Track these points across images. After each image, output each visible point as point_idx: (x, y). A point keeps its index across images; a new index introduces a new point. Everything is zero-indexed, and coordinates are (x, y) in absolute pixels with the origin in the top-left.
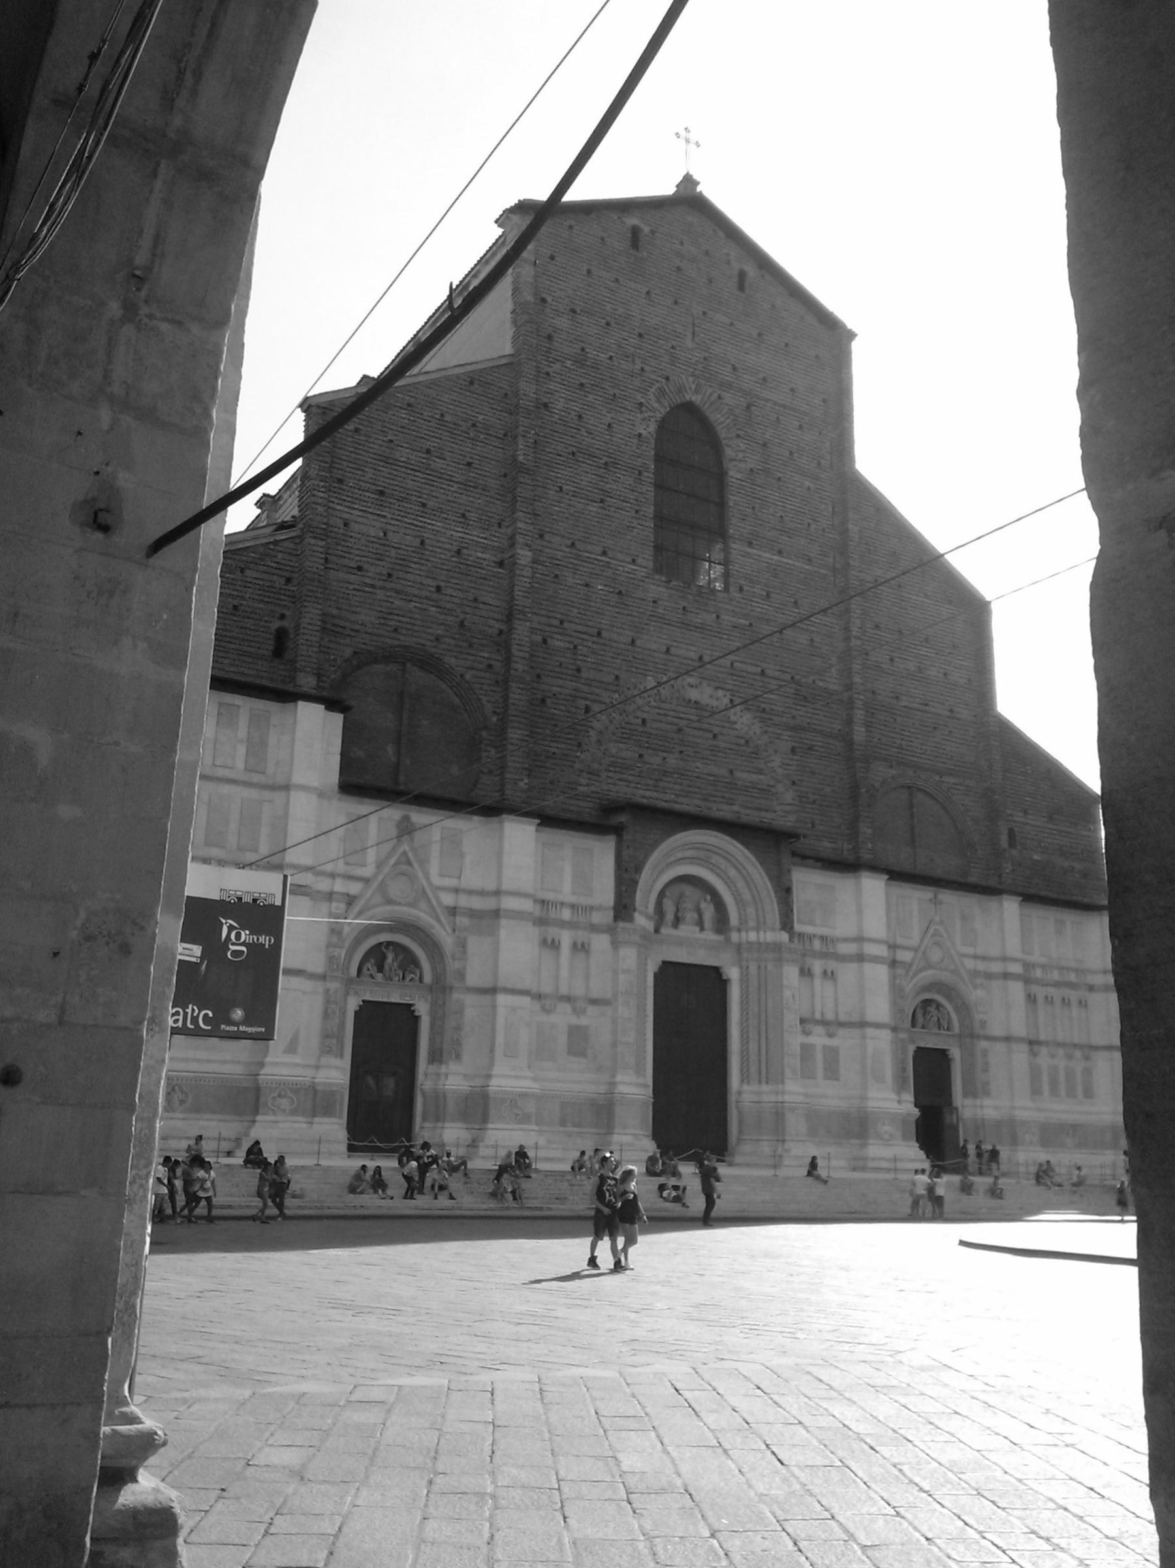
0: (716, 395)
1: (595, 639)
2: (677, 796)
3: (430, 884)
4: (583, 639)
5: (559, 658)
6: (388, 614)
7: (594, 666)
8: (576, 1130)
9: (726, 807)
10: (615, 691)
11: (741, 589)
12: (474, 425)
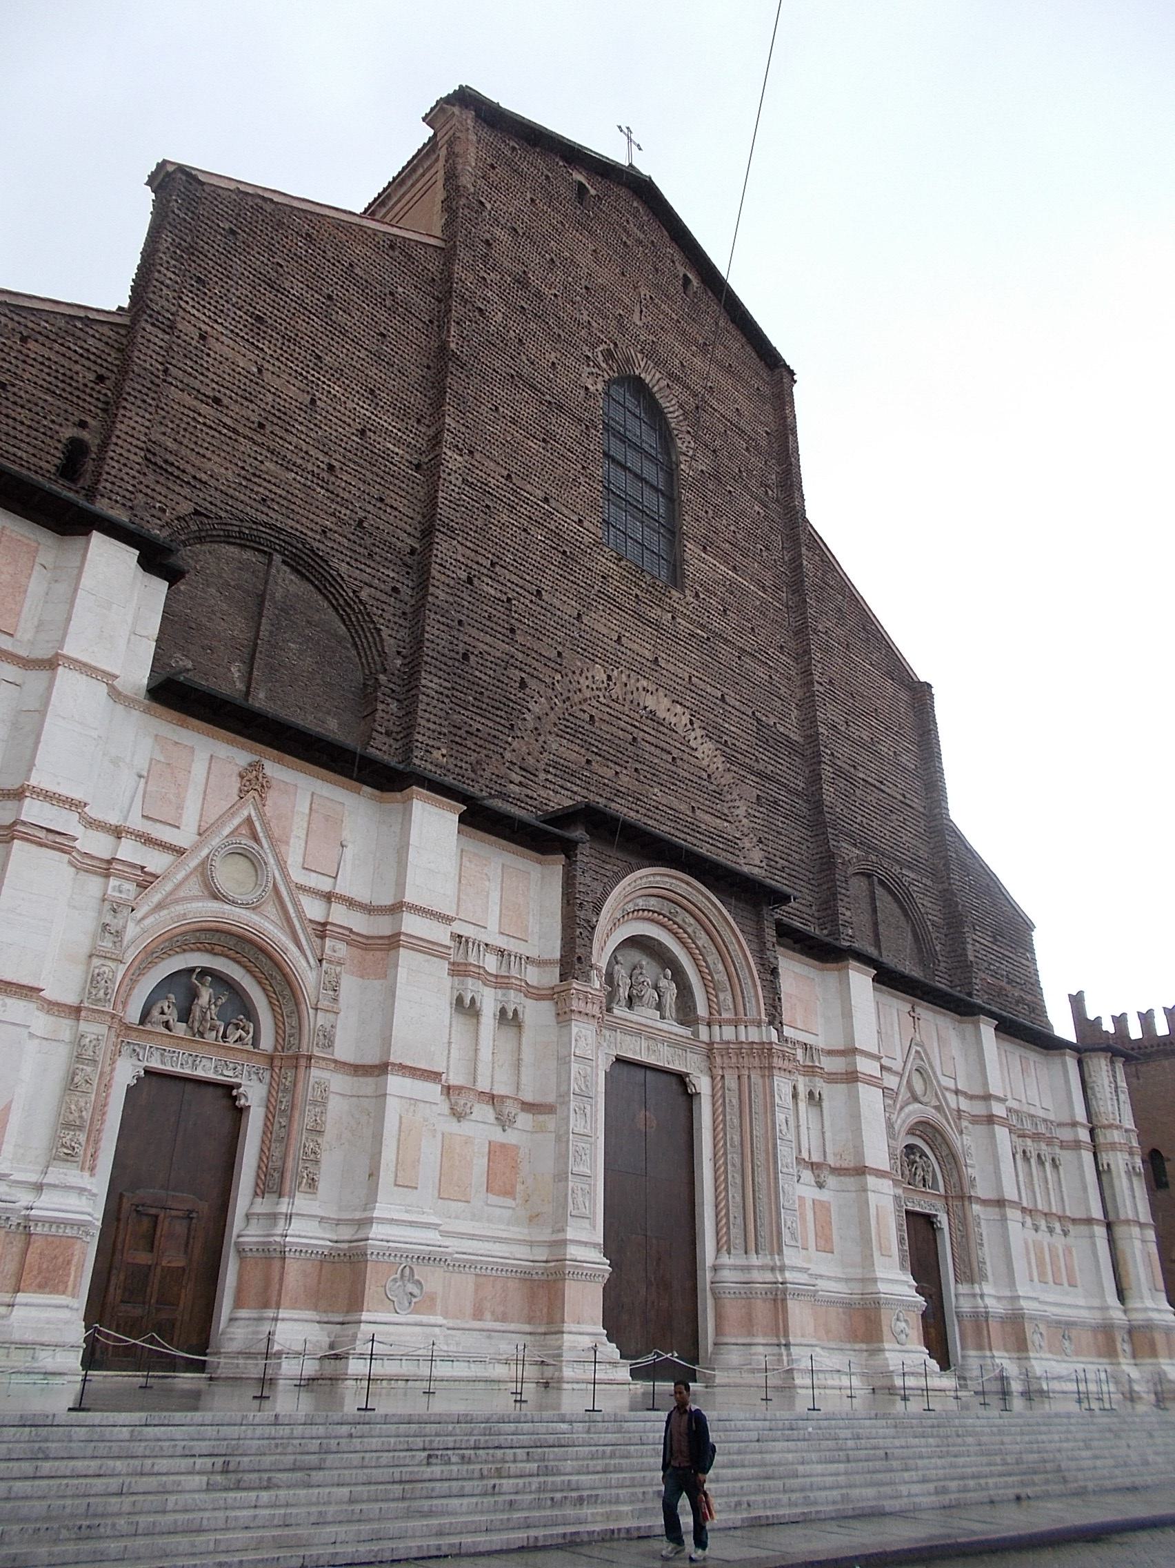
5: (490, 610)
6: (254, 475)
7: (532, 631)
8: (498, 1326)
11: (697, 595)
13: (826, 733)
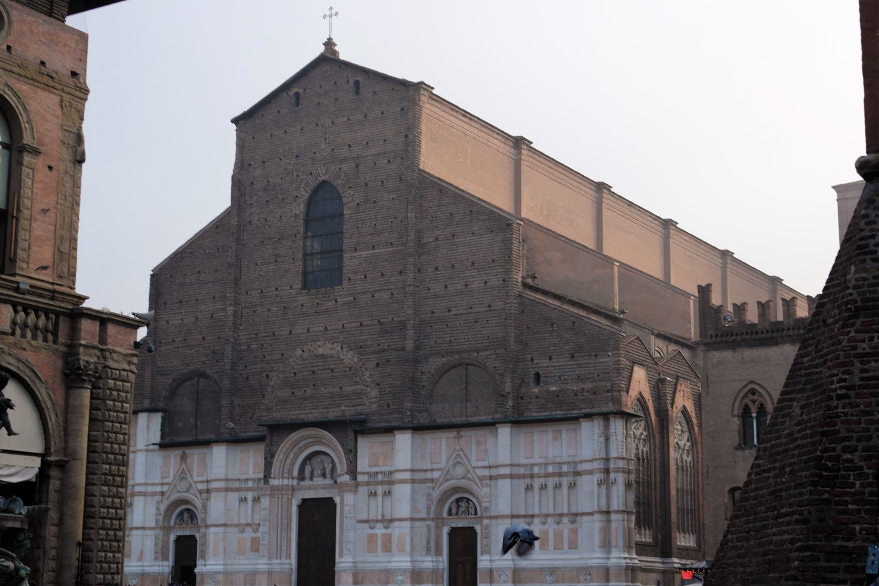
0: (338, 169)
1: (271, 338)
2: (311, 409)
3: (193, 480)
4: (265, 340)
9: (337, 409)
10: (280, 363)
11: (350, 279)
12: (218, 249)
13: (412, 312)
